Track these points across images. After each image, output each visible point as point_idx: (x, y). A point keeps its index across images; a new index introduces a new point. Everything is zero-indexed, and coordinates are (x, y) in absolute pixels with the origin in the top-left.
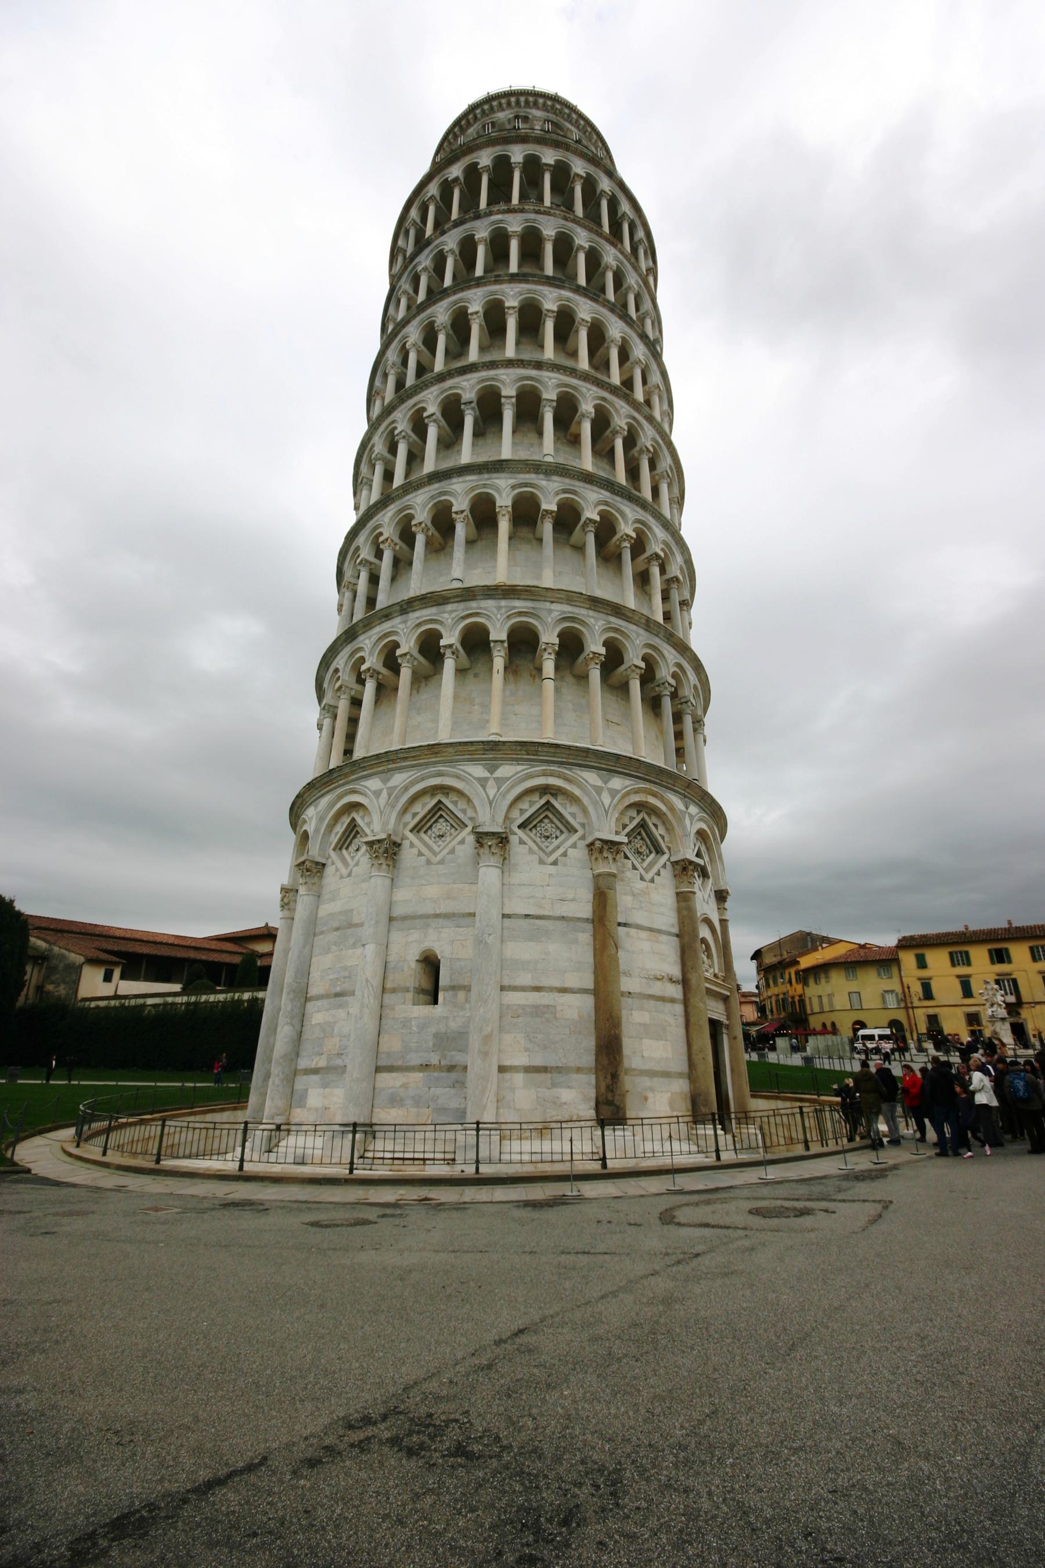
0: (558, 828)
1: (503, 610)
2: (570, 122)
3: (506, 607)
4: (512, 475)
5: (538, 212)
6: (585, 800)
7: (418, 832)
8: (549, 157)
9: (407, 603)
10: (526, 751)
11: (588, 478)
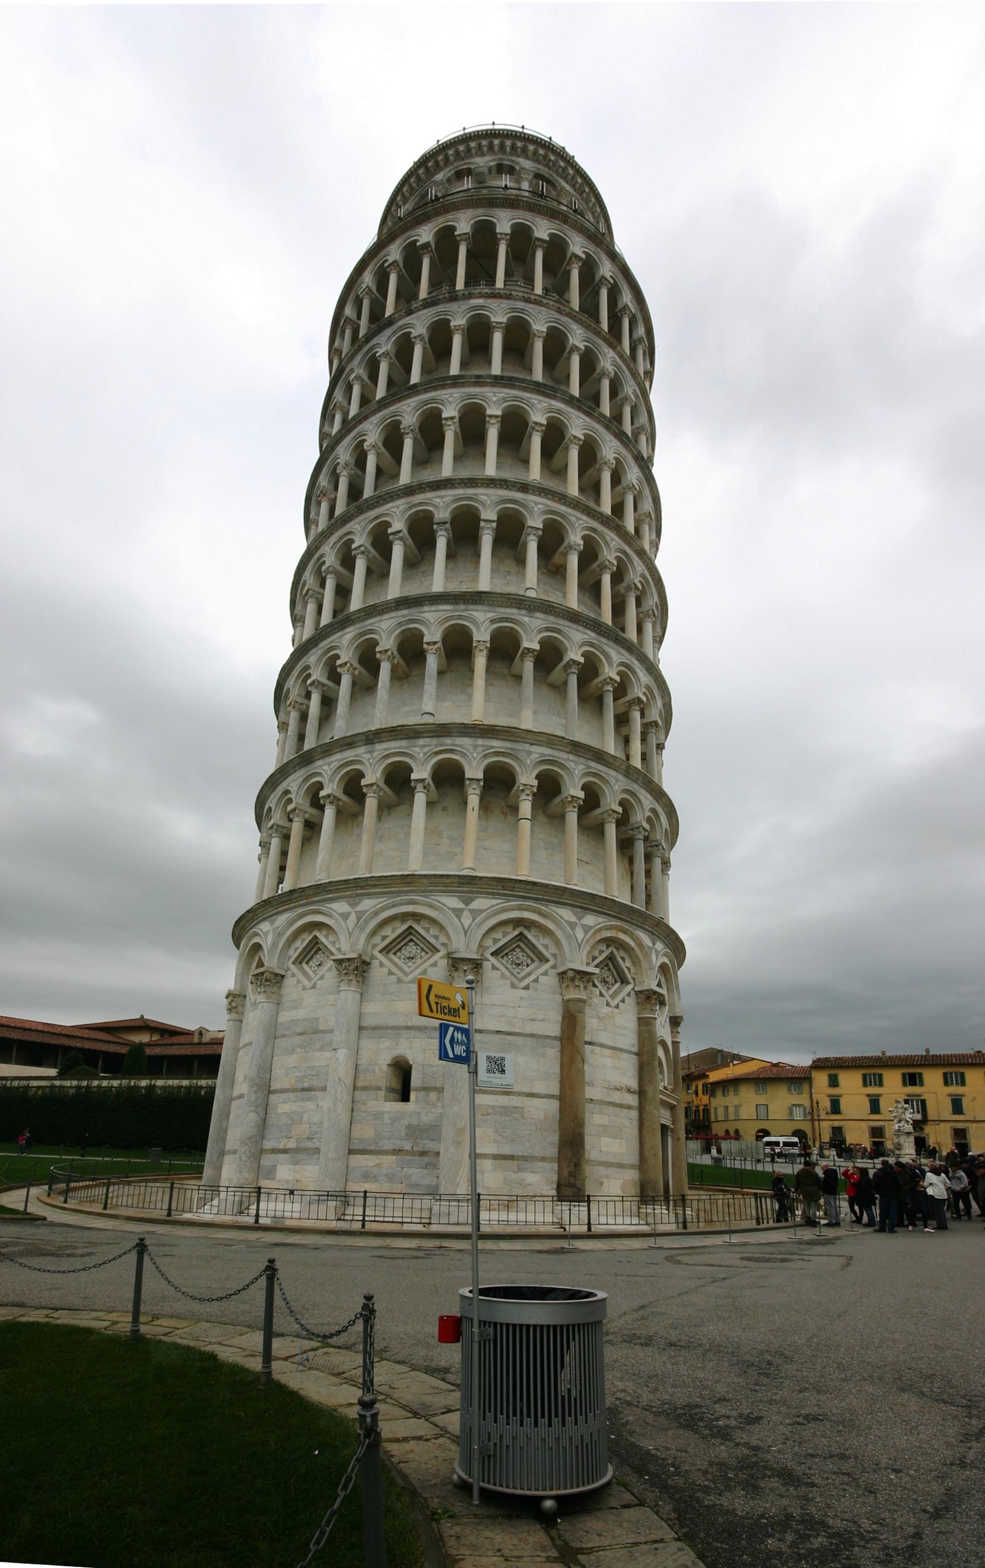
1: (480, 749)
3: (483, 746)
4: (491, 608)
6: (559, 934)
7: (387, 953)
8: (543, 230)
9: (374, 734)
11: (574, 617)
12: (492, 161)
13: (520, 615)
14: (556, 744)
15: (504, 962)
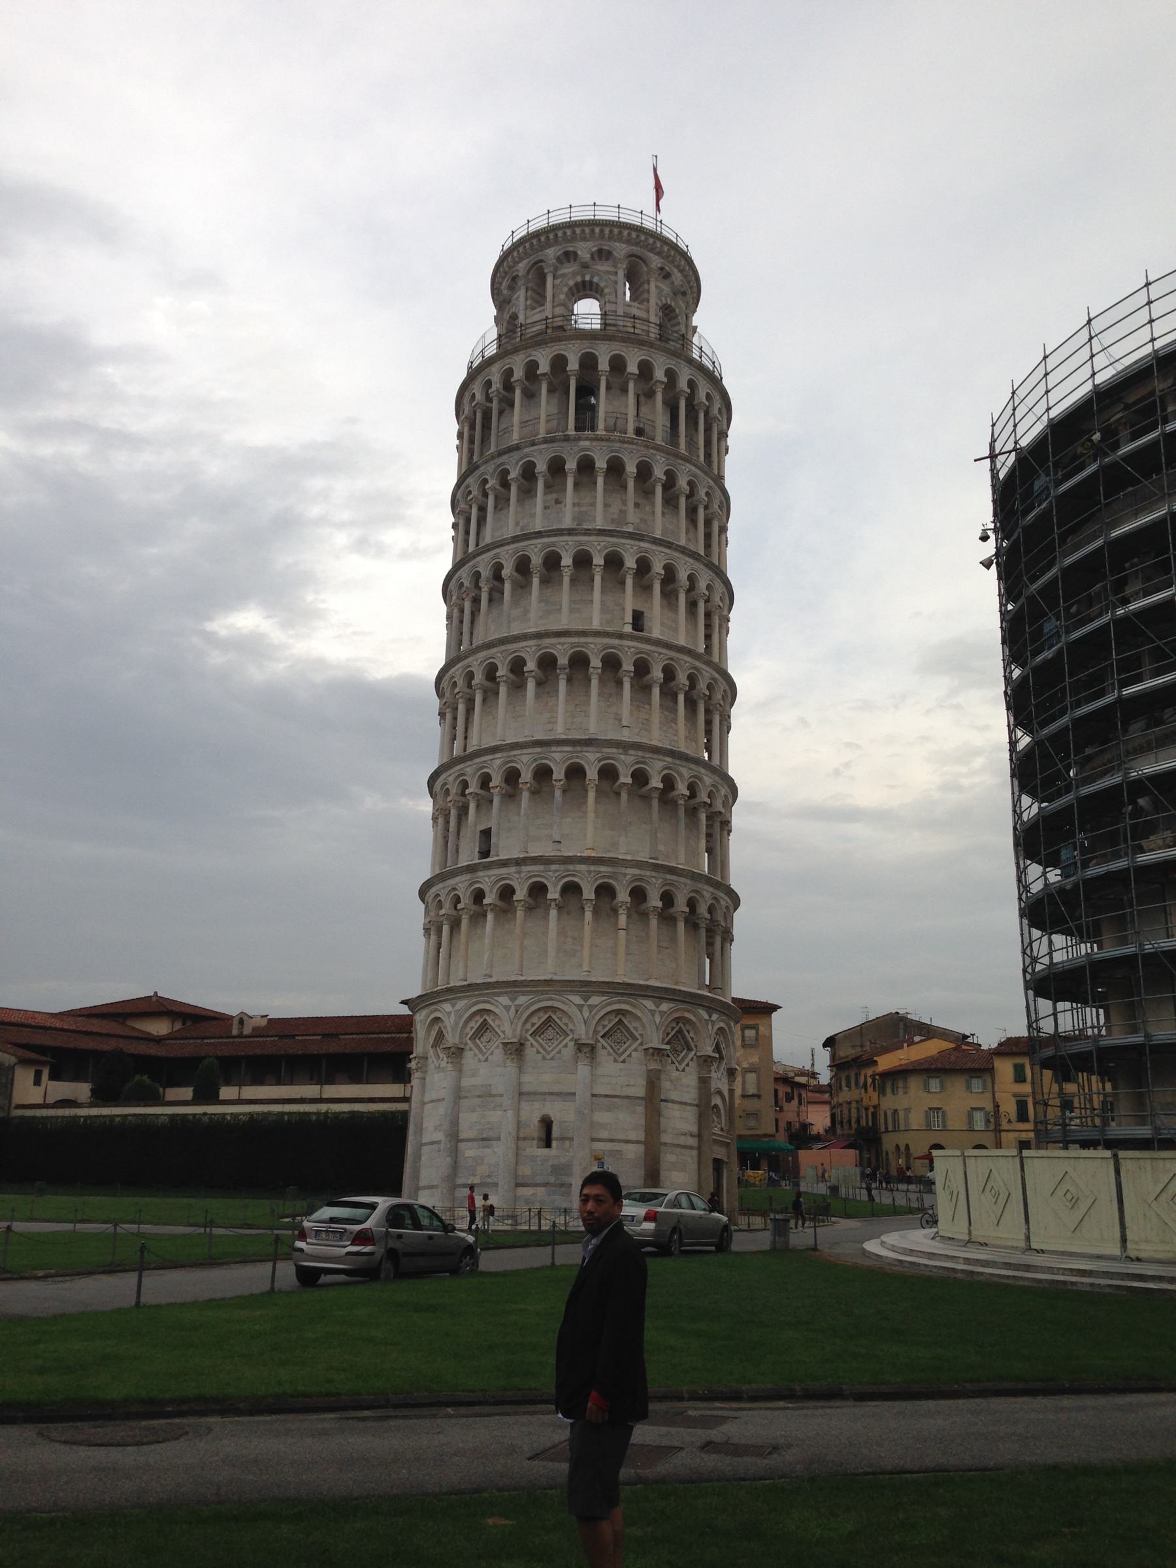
1: (593, 874)
2: (652, 250)
3: (594, 871)
6: (645, 1020)
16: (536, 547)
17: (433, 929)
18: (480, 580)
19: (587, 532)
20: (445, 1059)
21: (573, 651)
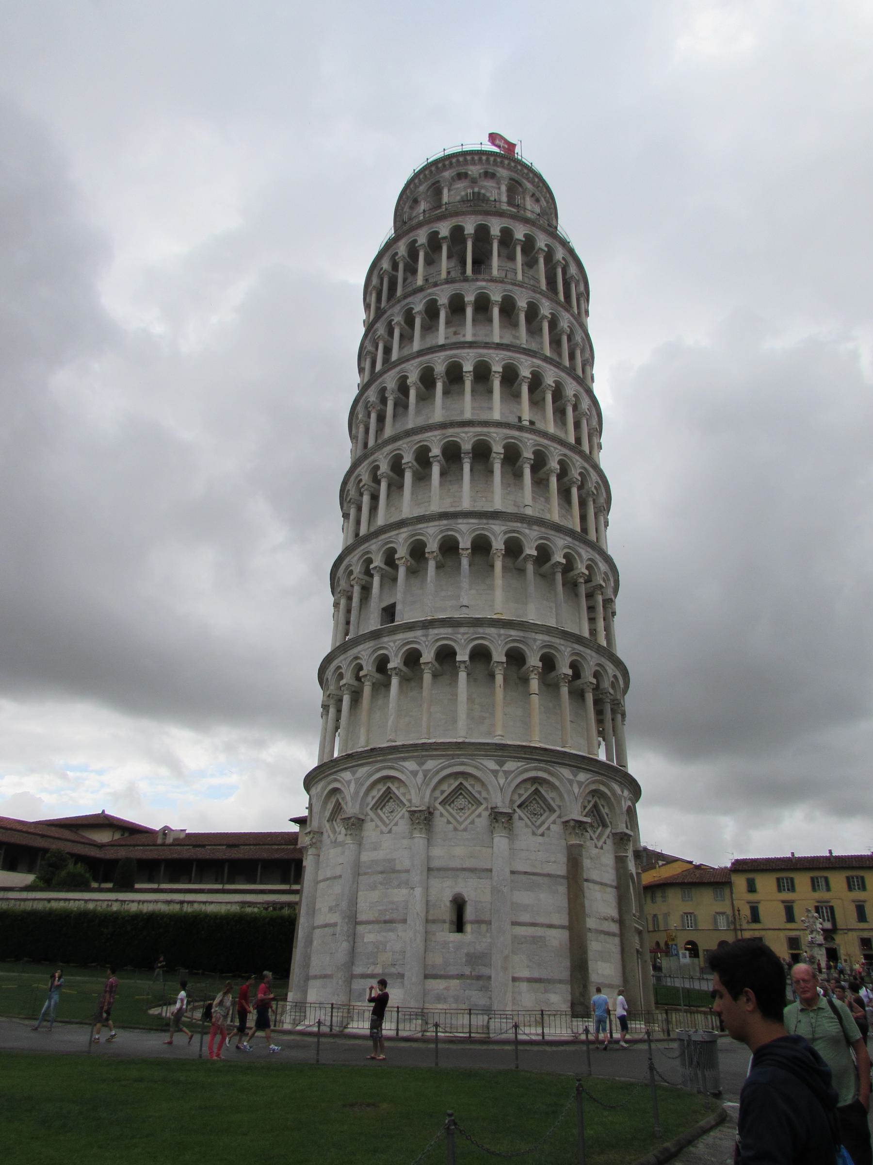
0: (542, 807)
1: (503, 637)
2: (527, 179)
5: (514, 284)
6: (562, 789)
7: (444, 804)
10: (524, 752)
12: (481, 169)
13: (523, 528)
14: (552, 633)
15: (525, 812)
16: (440, 358)
17: (332, 702)
18: (386, 392)
19: (487, 345)
20: (343, 831)
21: (476, 439)
